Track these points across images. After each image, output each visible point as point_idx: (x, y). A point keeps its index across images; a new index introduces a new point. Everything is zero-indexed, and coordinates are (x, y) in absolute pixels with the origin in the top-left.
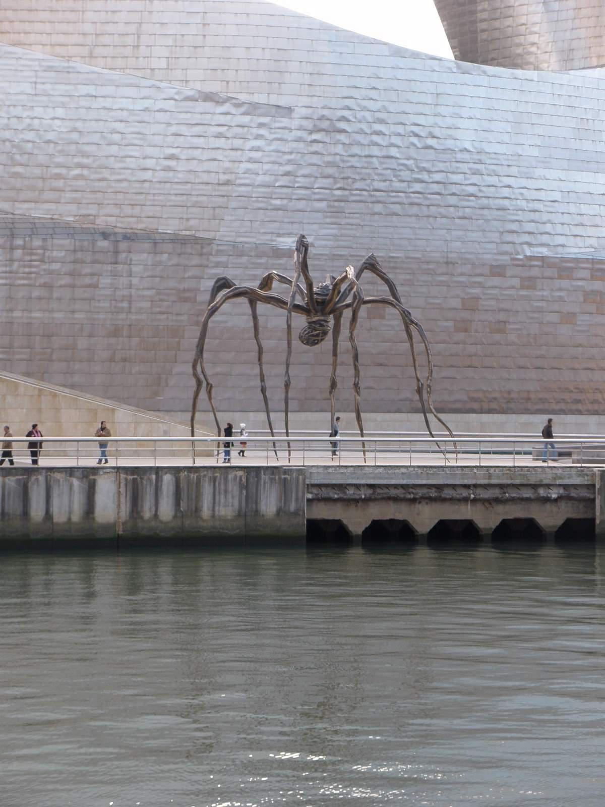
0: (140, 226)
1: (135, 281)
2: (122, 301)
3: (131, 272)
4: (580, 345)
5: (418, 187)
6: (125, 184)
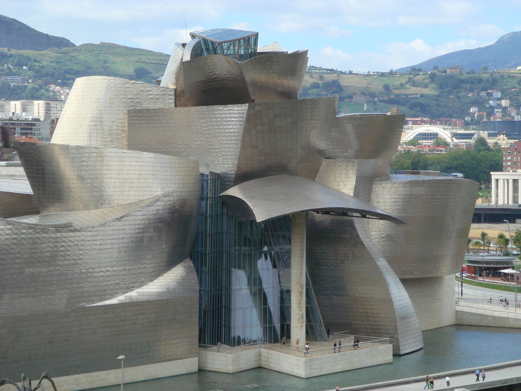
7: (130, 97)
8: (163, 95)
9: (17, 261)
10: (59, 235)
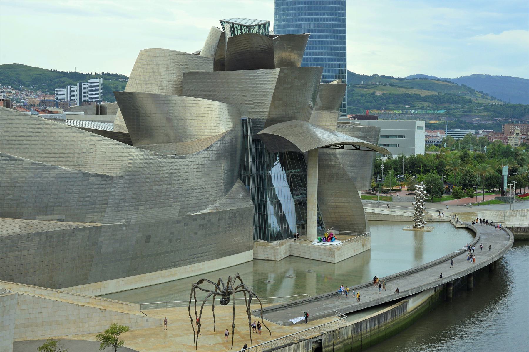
5: (158, 198)
7: (181, 64)
8: (205, 63)
9: (148, 180)
10: (173, 160)
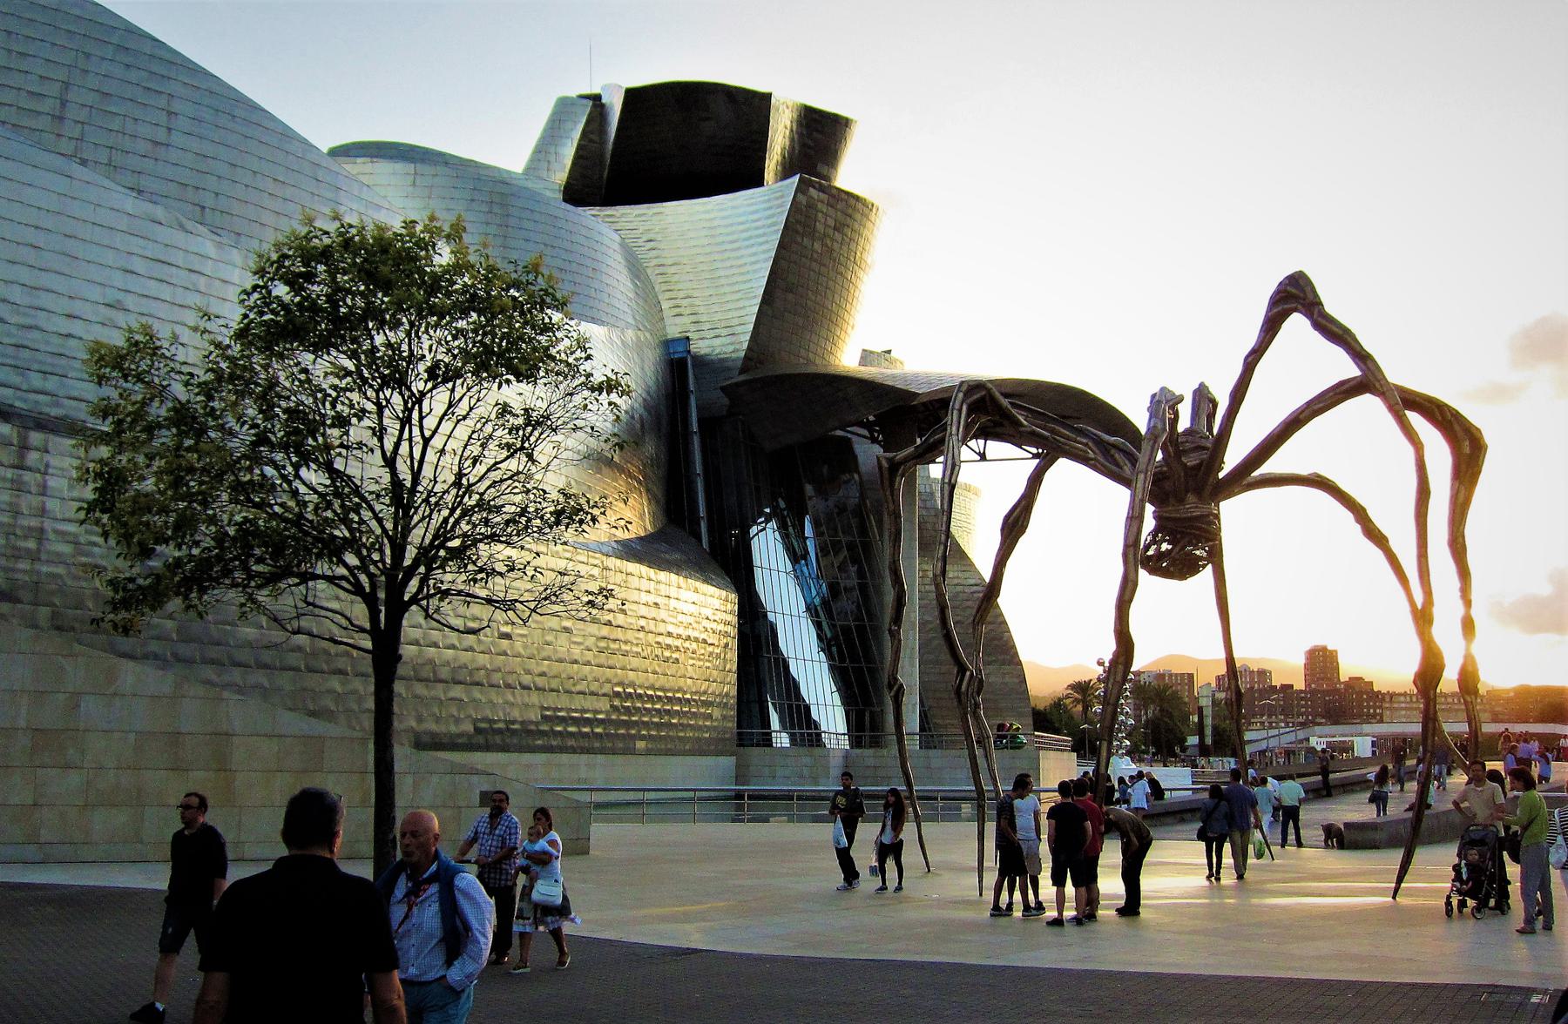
0: (55, 412)
1: (52, 504)
2: (26, 537)
3: (45, 486)
4: (576, 662)
6: (36, 335)
